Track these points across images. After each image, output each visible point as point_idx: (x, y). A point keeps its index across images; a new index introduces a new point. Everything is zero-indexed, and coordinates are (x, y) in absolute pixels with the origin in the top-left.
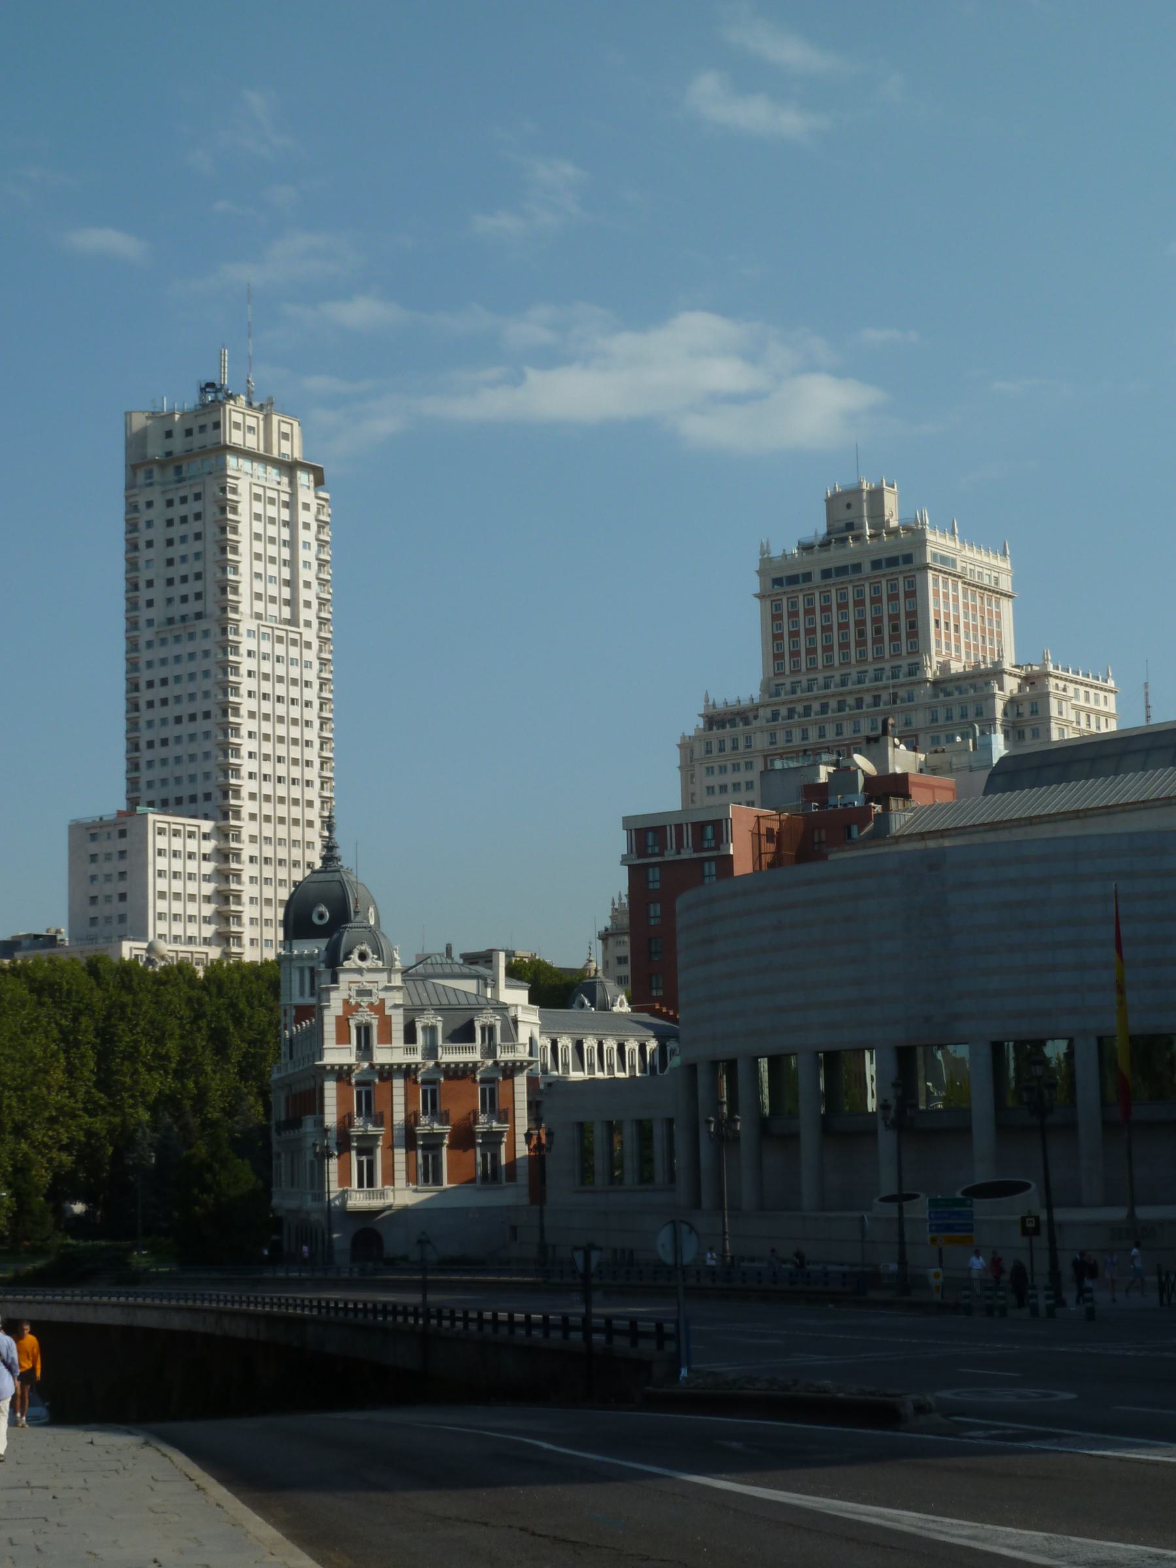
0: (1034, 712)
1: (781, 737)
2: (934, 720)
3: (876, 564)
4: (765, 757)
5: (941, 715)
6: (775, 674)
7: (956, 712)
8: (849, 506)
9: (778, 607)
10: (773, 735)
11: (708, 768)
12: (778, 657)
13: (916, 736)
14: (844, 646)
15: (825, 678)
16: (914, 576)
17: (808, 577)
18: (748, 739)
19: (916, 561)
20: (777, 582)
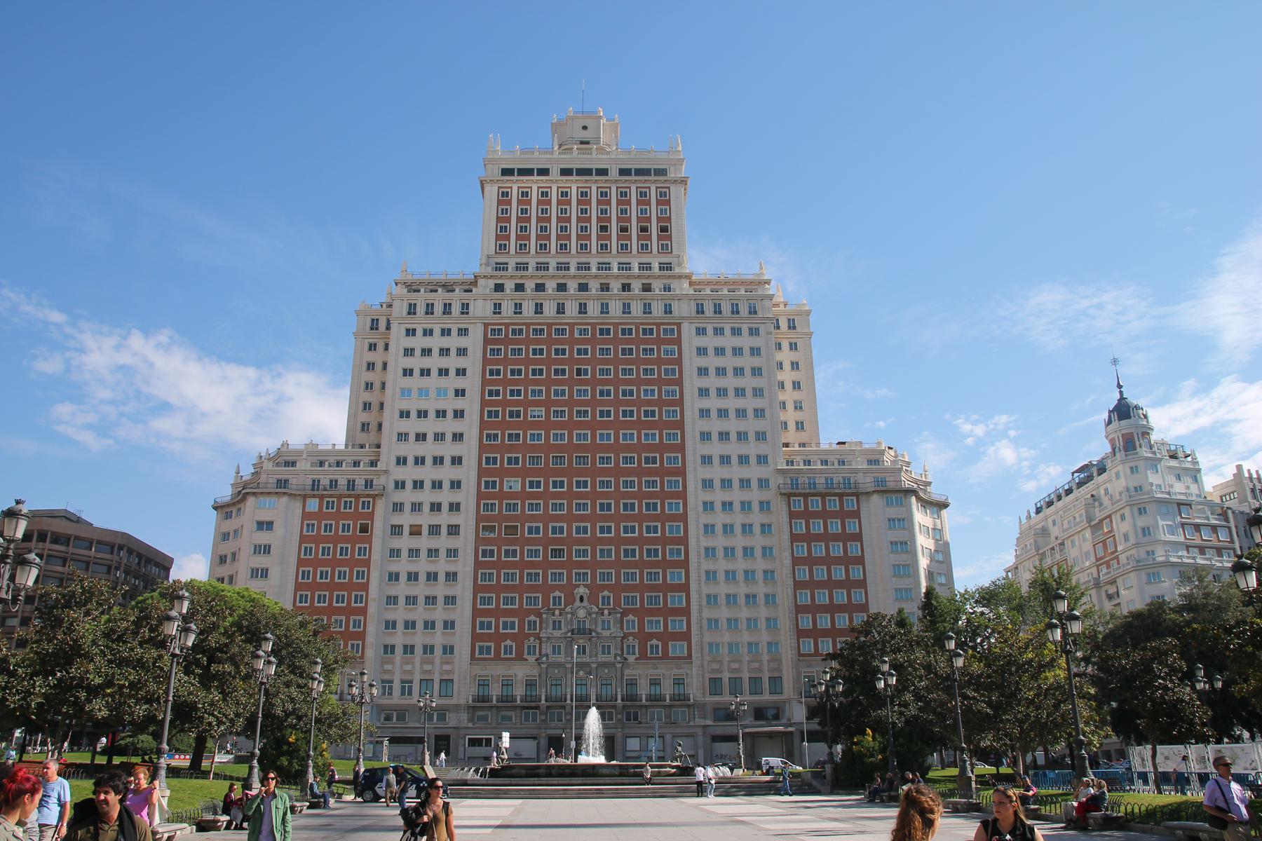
0: (792, 326)
1: (508, 309)
2: (700, 310)
3: (624, 172)
4: (486, 325)
5: (709, 309)
6: (496, 253)
7: (726, 309)
8: (585, 128)
9: (505, 194)
10: (497, 308)
11: (408, 330)
12: (502, 236)
13: (679, 325)
14: (584, 235)
15: (558, 264)
16: (669, 188)
17: (544, 172)
18: (465, 308)
19: (672, 175)
20: (507, 172)
